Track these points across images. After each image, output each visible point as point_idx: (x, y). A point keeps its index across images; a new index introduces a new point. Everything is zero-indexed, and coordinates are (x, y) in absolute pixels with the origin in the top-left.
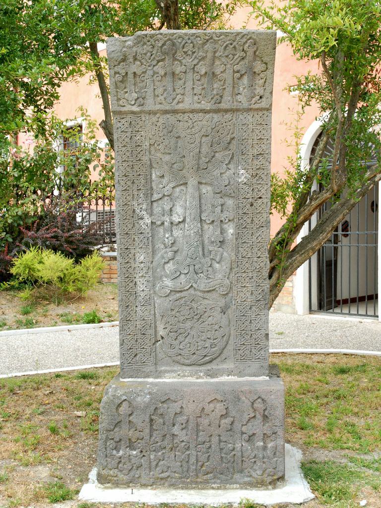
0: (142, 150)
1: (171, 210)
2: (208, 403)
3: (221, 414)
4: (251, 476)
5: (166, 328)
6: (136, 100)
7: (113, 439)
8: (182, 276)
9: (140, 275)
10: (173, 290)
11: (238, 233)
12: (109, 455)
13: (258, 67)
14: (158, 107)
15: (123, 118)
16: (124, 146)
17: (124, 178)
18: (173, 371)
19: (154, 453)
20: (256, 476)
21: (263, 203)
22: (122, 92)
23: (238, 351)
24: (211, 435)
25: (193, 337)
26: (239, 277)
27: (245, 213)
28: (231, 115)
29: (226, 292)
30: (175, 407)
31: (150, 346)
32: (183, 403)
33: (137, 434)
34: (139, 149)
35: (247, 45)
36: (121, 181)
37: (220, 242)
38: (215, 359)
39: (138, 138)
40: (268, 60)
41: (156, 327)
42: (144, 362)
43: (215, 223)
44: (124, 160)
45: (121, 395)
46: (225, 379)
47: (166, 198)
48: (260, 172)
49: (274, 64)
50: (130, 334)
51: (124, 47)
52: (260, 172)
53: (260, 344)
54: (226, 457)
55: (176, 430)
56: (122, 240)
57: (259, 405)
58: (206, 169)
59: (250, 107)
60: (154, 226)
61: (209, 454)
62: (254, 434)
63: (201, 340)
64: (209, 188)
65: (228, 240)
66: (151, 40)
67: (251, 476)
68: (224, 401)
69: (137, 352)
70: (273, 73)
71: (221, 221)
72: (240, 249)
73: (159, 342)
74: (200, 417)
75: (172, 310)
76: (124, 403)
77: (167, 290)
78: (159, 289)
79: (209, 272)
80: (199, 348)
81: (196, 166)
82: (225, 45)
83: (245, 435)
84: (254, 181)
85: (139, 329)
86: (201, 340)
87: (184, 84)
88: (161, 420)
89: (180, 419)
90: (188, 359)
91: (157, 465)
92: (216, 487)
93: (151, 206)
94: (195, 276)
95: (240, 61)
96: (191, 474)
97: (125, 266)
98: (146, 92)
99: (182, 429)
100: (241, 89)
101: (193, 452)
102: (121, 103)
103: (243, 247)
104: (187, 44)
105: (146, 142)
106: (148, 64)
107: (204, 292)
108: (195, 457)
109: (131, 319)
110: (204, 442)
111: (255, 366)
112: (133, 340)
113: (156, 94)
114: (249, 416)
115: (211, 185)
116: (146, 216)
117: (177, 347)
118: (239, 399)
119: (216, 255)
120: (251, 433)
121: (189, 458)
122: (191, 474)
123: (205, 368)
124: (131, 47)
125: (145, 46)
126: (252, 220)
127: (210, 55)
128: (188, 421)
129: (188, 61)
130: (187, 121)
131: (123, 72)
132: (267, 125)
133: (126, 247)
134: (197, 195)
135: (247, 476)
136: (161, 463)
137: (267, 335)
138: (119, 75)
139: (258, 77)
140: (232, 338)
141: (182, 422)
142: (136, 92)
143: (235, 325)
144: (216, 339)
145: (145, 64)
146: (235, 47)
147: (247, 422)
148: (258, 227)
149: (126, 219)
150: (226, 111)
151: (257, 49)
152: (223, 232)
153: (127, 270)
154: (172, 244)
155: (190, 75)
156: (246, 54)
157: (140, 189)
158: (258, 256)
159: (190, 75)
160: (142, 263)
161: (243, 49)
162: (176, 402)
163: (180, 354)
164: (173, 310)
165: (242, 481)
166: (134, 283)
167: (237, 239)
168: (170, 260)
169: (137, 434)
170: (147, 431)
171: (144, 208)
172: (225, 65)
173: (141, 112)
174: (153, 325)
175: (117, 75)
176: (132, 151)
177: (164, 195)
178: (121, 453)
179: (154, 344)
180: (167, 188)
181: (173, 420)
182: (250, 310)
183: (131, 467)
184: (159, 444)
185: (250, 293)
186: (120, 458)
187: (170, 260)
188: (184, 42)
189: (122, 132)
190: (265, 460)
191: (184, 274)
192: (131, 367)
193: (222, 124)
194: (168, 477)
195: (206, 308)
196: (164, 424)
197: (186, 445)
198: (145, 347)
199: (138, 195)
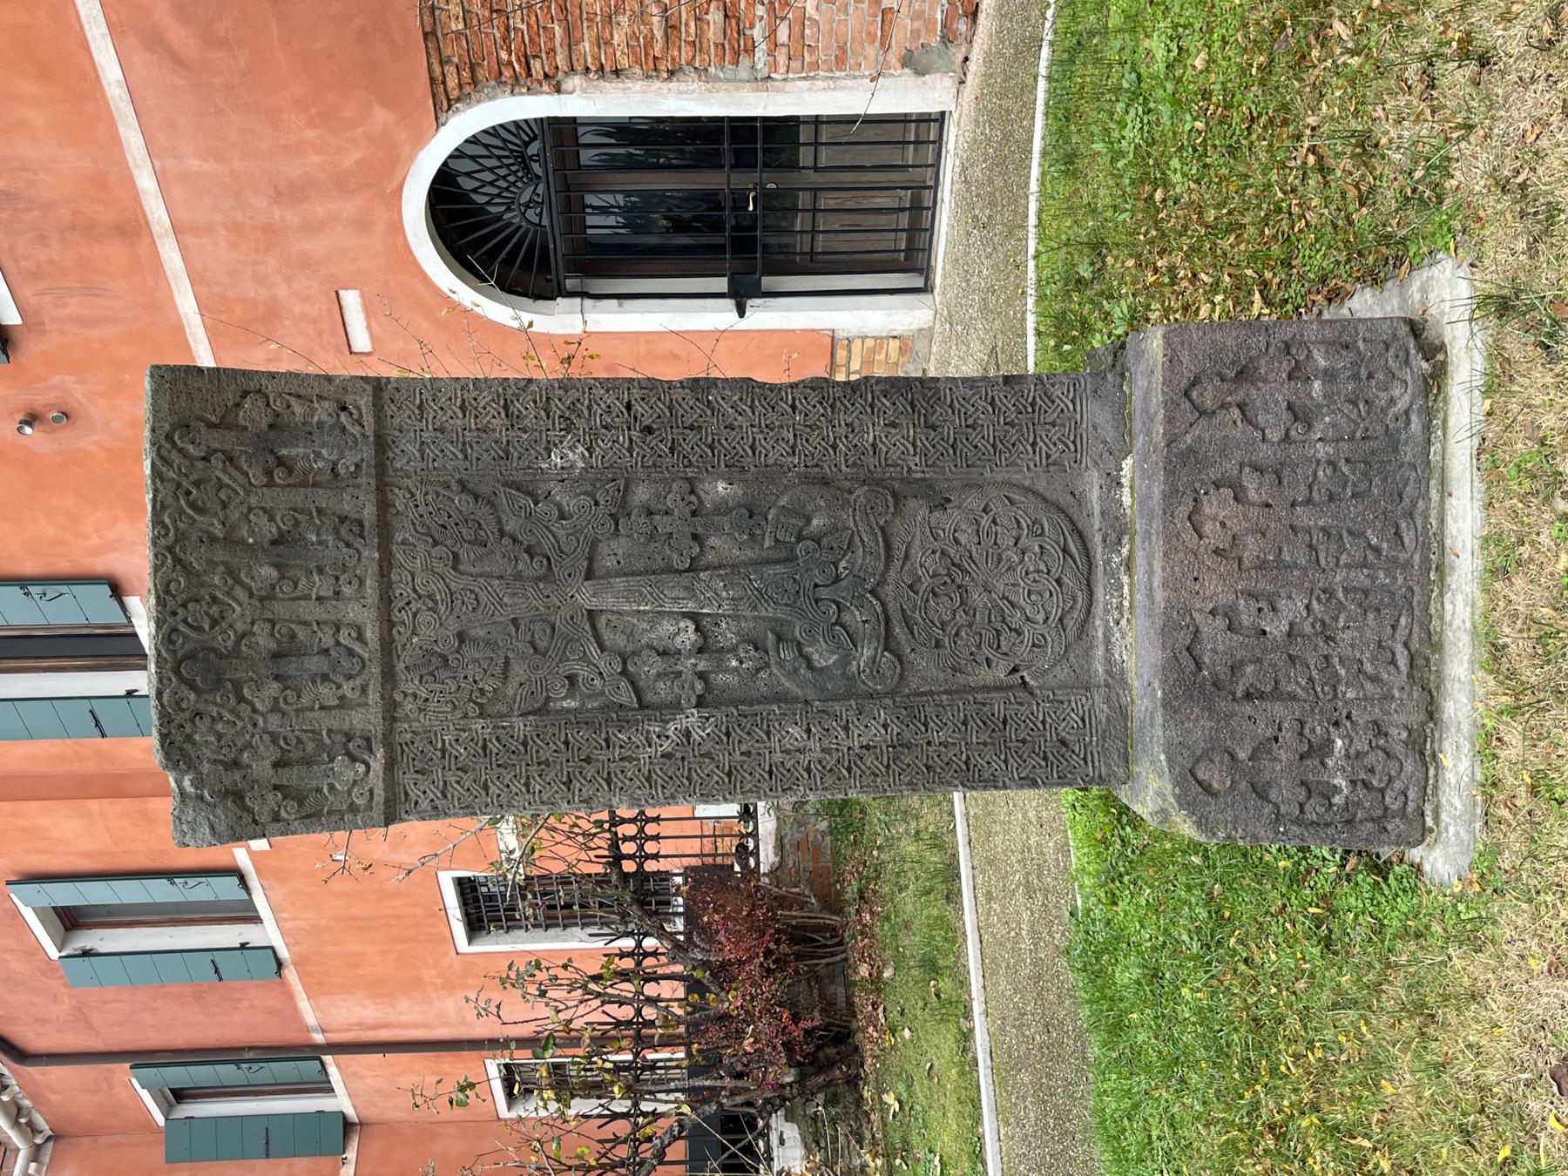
0: (498, 739)
1: (664, 653)
2: (1201, 537)
4: (1407, 412)
5: (987, 659)
7: (1301, 805)
8: (846, 618)
10: (882, 641)
11: (726, 466)
12: (1347, 816)
13: (253, 414)
14: (374, 697)
15: (406, 794)
16: (486, 788)
19: (1342, 688)
20: (1407, 398)
21: (643, 399)
22: (331, 798)
23: (1050, 461)
24: (1292, 527)
26: (847, 461)
27: (672, 450)
28: (397, 491)
29: (889, 498)
30: (1212, 629)
31: (1038, 704)
32: (1201, 610)
34: (494, 746)
35: (191, 448)
36: (585, 794)
37: (751, 517)
38: (1072, 522)
41: (985, 688)
42: (1083, 720)
43: (700, 530)
47: (631, 668)
48: (557, 407)
49: (244, 373)
50: (1005, 761)
52: (557, 407)
53: (1034, 397)
54: (1354, 484)
55: (1276, 628)
56: (748, 787)
57: (1207, 395)
58: (549, 559)
59: (372, 439)
60: (709, 698)
61: (1345, 534)
62: (1290, 407)
63: (1022, 561)
64: (603, 549)
65: (745, 494)
66: (178, 720)
67: (1407, 412)
68: (1194, 495)
69: (1055, 739)
70: (273, 376)
71: (694, 513)
72: (771, 461)
73: (1027, 679)
74: (1240, 560)
76: (1200, 775)
77: (884, 659)
78: (883, 682)
79: (835, 546)
80: (1042, 567)
83: (1293, 433)
84: (581, 424)
85: (990, 737)
86: (1022, 561)
88: (1250, 669)
89: (1244, 617)
91: (1374, 679)
93: (652, 709)
94: (844, 583)
95: (240, 469)
96: (1400, 580)
97: (818, 779)
98: (330, 731)
99: (1274, 609)
100: (321, 464)
101: (1338, 579)
102: (360, 802)
107: (889, 558)
110: (1311, 546)
112: (1020, 753)
113: (336, 702)
114: (1239, 423)
115: (594, 544)
116: (681, 722)
117: (1041, 629)
120: (1286, 416)
121: (1355, 590)
122: (1400, 580)
123: (1100, 550)
124: (198, 783)
125: (197, 737)
126: (691, 428)
127: (221, 555)
128: (1249, 595)
129: (239, 614)
130: (415, 615)
131: (273, 799)
133: (766, 776)
134: (620, 583)
135: (1408, 423)
136: (1368, 667)
137: (1007, 380)
138: (282, 811)
140: (1016, 478)
141: (1253, 611)
142: (332, 760)
143: (981, 470)
144: (1018, 522)
146: (197, 484)
147: (1256, 427)
148: (709, 412)
149: (688, 779)
150: (384, 505)
151: (202, 419)
152: (723, 509)
153: (831, 770)
154: (756, 649)
156: (215, 451)
157: (607, 740)
158: (789, 410)
159: (281, 610)
160: (809, 731)
161: (204, 459)
162: (1197, 631)
163: (1061, 619)
164: (937, 641)
166: (865, 751)
168: (801, 654)
169: (1287, 735)
170: (1278, 709)
171: (657, 729)
172: (250, 509)
173: (388, 743)
174: (980, 697)
176: (499, 766)
177: (624, 673)
178: (1340, 781)
179: (1032, 694)
181: (1247, 636)
182: (940, 430)
183: (1379, 752)
185: (893, 431)
186: (1353, 783)
187: (801, 654)
188: (182, 628)
189: (445, 796)
190: (1363, 373)
191: (839, 612)
192: (1096, 755)
193: (422, 516)
194: (1406, 645)
196: (1259, 661)
197: (1318, 599)
198: (1041, 718)
199: (621, 747)
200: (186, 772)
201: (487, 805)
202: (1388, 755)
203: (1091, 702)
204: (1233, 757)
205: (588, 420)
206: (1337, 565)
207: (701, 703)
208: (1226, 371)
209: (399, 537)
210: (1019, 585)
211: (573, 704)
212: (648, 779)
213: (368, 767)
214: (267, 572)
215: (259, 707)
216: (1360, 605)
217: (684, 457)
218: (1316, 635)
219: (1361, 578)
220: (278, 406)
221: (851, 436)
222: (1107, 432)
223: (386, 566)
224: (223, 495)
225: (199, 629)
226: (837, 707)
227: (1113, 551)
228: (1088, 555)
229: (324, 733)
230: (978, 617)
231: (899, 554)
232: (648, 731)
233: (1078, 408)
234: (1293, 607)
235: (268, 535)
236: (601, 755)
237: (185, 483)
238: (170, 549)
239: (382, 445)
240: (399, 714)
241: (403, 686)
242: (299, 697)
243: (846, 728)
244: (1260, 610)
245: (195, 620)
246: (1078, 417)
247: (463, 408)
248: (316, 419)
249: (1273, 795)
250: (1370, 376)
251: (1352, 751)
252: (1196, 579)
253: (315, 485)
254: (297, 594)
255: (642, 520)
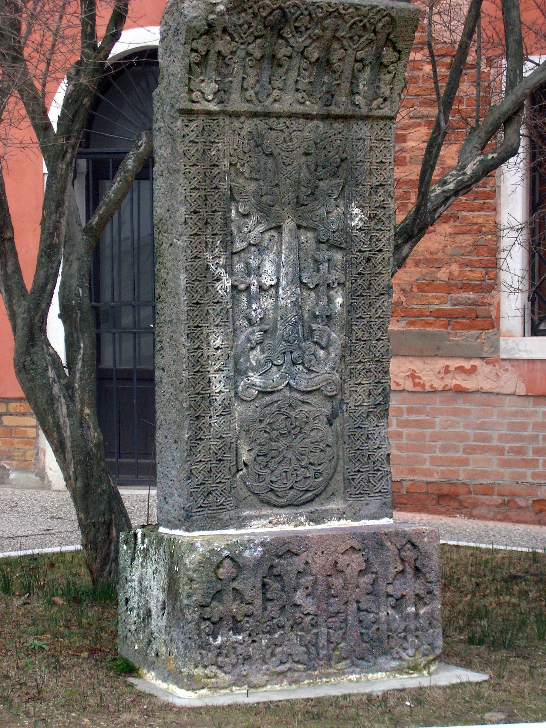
0: (219, 173)
2: (342, 554)
3: (359, 569)
4: (400, 658)
6: (215, 94)
9: (216, 367)
10: (263, 390)
13: (388, 55)
14: (246, 107)
15: (191, 121)
16: (194, 165)
17: (194, 216)
18: (261, 517)
21: (384, 258)
22: (197, 80)
24: (347, 602)
25: (290, 463)
26: (353, 369)
27: (359, 274)
31: (229, 479)
32: (308, 556)
33: (245, 608)
34: (215, 171)
35: (380, 25)
36: (189, 221)
39: (213, 153)
40: (404, 47)
41: (237, 449)
42: (221, 505)
44: (193, 187)
45: (221, 550)
46: (334, 524)
48: (380, 212)
51: (212, 12)
54: (367, 633)
56: (190, 313)
57: (409, 553)
59: (370, 114)
62: (403, 596)
63: (302, 467)
64: (310, 235)
65: (336, 314)
66: (255, 6)
67: (400, 658)
68: (362, 549)
69: (211, 489)
71: (328, 285)
72: (354, 327)
75: (261, 421)
79: (312, 363)
81: (295, 200)
82: (352, 21)
83: (390, 599)
86: (302, 467)
87: (286, 73)
90: (283, 497)
92: (355, 680)
98: (231, 82)
101: (322, 629)
102: (194, 95)
103: (358, 324)
104: (301, 16)
105: (225, 160)
106: (241, 41)
108: (325, 637)
109: (203, 437)
111: (374, 504)
113: (245, 87)
114: (396, 570)
115: (314, 229)
116: (225, 277)
118: (382, 545)
119: (321, 337)
120: (399, 594)
123: (305, 510)
124: (221, 14)
125: (243, 14)
127: (328, 34)
129: (300, 41)
130: (281, 130)
131: (203, 50)
132: (389, 141)
133: (196, 324)
138: (196, 54)
139: (385, 71)
140: (341, 462)
141: (308, 584)
142: (216, 82)
145: (237, 40)
146: (364, 26)
148: (377, 294)
150: (337, 117)
152: (330, 301)
153: (198, 361)
154: (261, 319)
155: (296, 61)
157: (216, 234)
158: (378, 338)
159: (296, 61)
162: (297, 555)
165: (388, 667)
166: (208, 380)
167: (349, 312)
169: (245, 608)
170: (258, 602)
171: (221, 263)
172: (346, 50)
173: (223, 112)
175: (194, 54)
176: (205, 173)
177: (250, 245)
178: (220, 640)
180: (255, 232)
184: (275, 621)
185: (366, 394)
188: (299, 12)
189: (190, 142)
192: (202, 513)
194: (290, 669)
195: (307, 417)
197: (313, 619)
199: (213, 242)
200: (227, 8)
201: (185, 166)
202: (234, 666)
203: (230, 509)
204: (234, 579)
205: (374, 229)
206: (329, 628)
207: (234, 287)
208: (419, 561)
209: (321, 124)
210: (290, 466)
211: (233, 216)
212: (196, 257)
213: (209, 101)
214: (315, 56)
215: (251, 46)
216: (309, 642)
217: (356, 281)
218: (295, 620)
219: (323, 642)
220: (391, 68)
221: (365, 371)
222: (365, 511)
223: (307, 117)
224: (356, 38)
225: (296, 20)
226: (231, 365)
227: (307, 518)
228: (304, 504)
229: (230, 79)
230: (274, 443)
231: (306, 397)
232: (220, 257)
233: (376, 495)
234: (309, 605)
235: (332, 58)
236: (209, 231)
237: (365, 21)
238: (337, 10)
239: (366, 118)
240: (234, 119)
241: (247, 122)
242: (250, 67)
243: (220, 370)
244: (307, 588)
245: (301, 19)
246: (372, 495)
247: (381, 162)
248: (383, 86)
249: (215, 603)
250: (417, 637)
251: (236, 645)
252: (323, 552)
253: (352, 83)
254: (302, 70)
255: (326, 257)
